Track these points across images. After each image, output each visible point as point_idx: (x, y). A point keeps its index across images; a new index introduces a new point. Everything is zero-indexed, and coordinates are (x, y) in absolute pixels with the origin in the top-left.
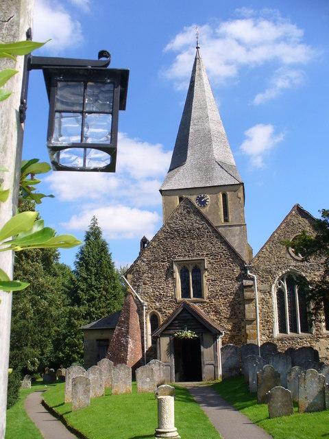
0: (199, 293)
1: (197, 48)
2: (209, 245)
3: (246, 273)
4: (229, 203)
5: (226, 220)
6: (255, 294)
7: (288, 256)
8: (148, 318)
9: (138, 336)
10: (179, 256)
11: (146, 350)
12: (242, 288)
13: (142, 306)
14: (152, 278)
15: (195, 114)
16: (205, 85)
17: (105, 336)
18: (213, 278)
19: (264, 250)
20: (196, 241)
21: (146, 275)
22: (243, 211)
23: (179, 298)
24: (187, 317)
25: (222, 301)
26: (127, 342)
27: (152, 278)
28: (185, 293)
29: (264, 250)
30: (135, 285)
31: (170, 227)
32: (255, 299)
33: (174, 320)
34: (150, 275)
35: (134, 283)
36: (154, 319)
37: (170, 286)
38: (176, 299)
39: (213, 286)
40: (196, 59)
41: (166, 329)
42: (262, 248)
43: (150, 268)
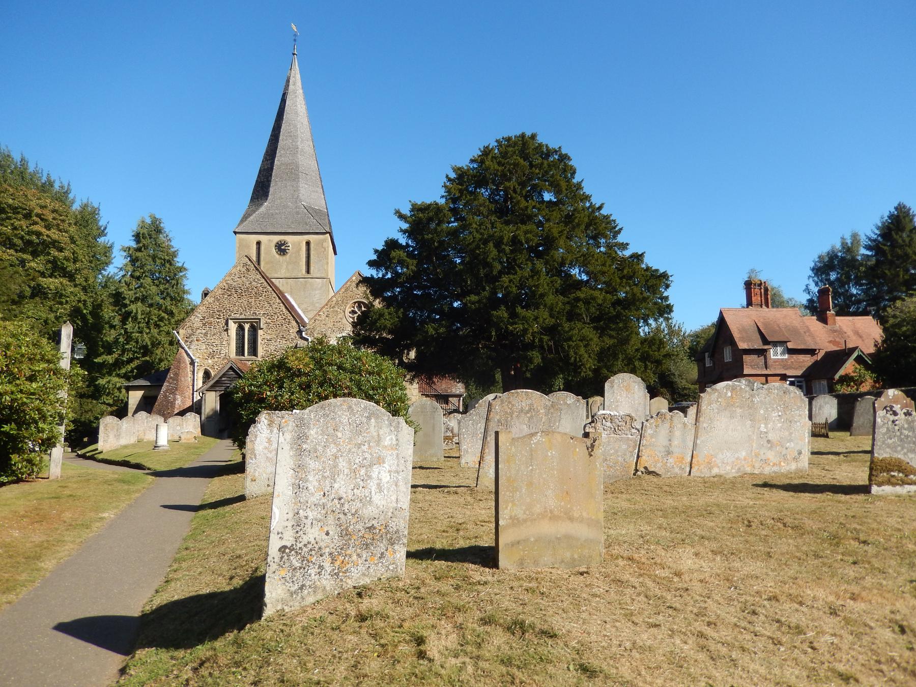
0: (254, 351)
5: (308, 272)
7: (344, 321)
14: (206, 334)
17: (152, 393)
21: (199, 331)
22: (328, 263)
26: (175, 400)
27: (206, 334)
28: (240, 351)
33: (221, 378)
36: (207, 375)
43: (204, 324)
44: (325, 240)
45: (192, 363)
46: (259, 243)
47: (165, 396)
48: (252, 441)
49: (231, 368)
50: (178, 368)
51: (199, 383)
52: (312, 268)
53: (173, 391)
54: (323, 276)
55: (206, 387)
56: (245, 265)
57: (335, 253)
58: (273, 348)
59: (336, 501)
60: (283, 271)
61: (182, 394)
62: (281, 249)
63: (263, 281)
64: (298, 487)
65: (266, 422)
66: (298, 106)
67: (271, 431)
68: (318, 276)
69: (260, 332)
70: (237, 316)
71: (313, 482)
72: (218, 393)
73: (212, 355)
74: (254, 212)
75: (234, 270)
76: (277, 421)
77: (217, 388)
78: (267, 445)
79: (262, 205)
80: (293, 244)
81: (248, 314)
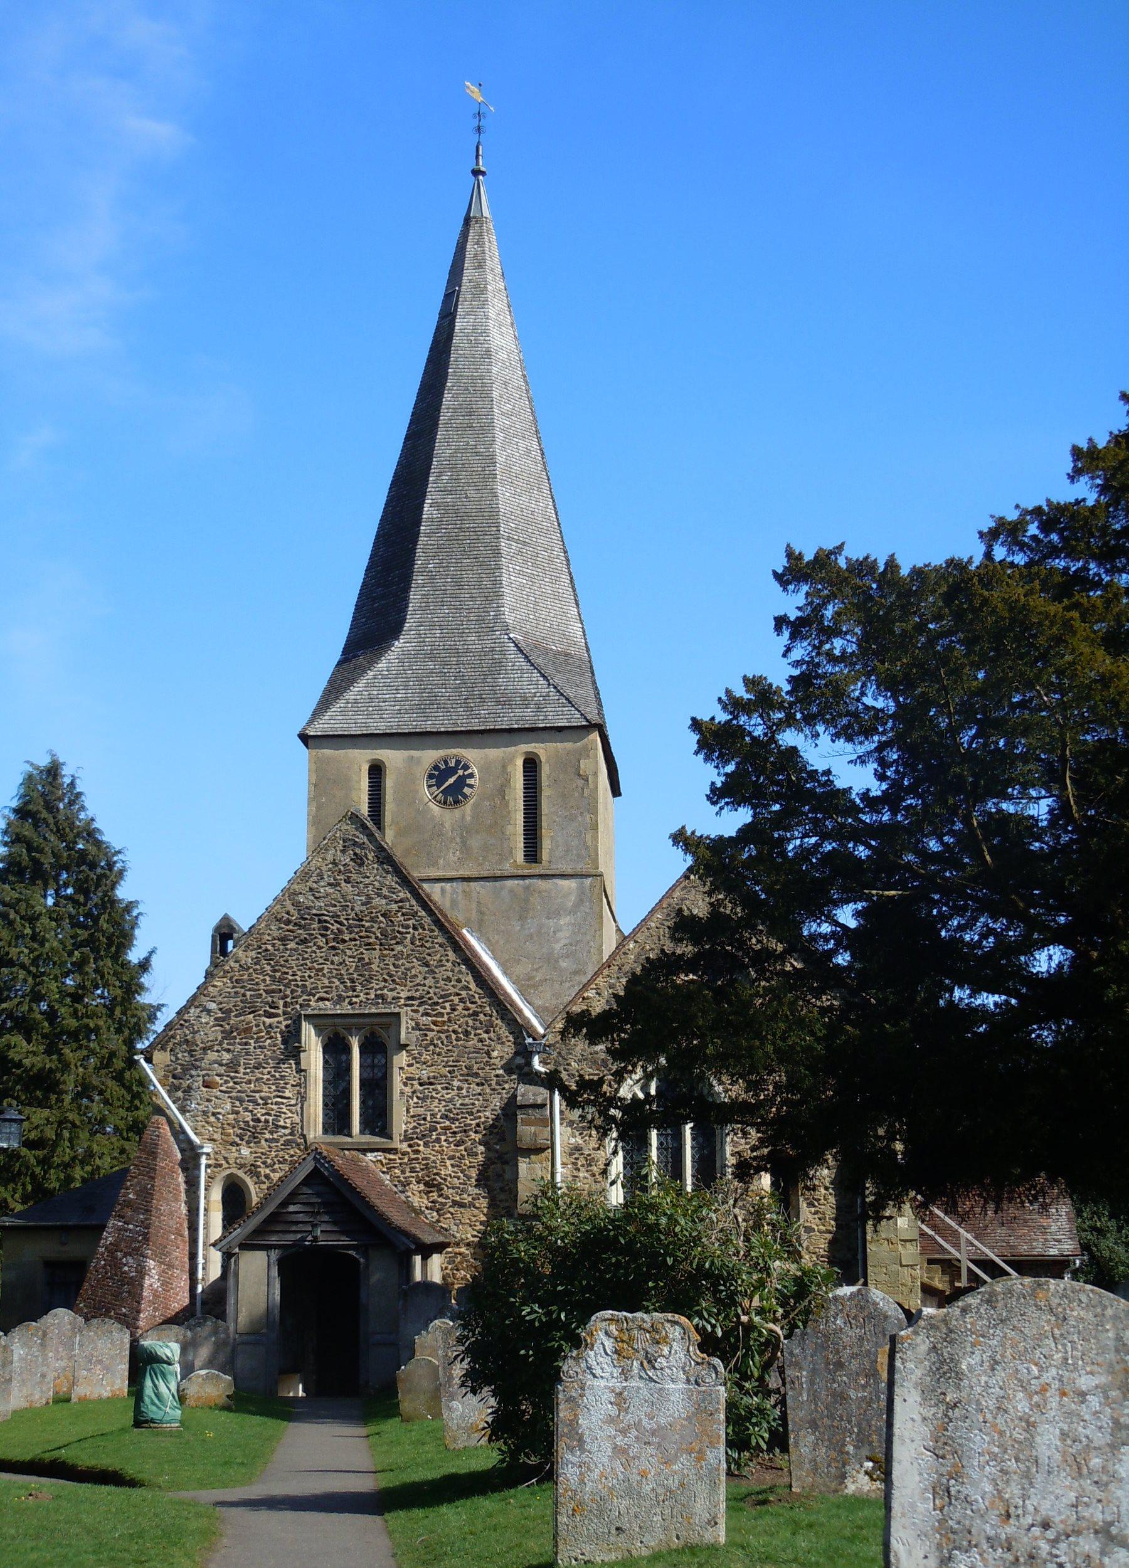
0: (378, 1119)
1: (476, 173)
2: (418, 969)
3: (529, 1063)
4: (547, 793)
6: (552, 1132)
8: (217, 1195)
9: (180, 1254)
10: (322, 999)
11: (200, 1289)
12: (511, 1109)
13: (198, 1156)
14: (233, 1066)
15: (444, 447)
16: (494, 332)
17: (73, 1250)
18: (425, 1074)
19: (590, 994)
20: (376, 954)
21: (212, 1056)
22: (595, 827)
23: (315, 1131)
24: (328, 1189)
26: (142, 1272)
27: (233, 1066)
28: (337, 1119)
29: (590, 994)
30: (177, 1089)
31: (296, 904)
32: (552, 1147)
33: (284, 1204)
34: (226, 1056)
35: (176, 1080)
37: (287, 1094)
38: (304, 1136)
39: (423, 1099)
40: (467, 221)
41: (259, 1232)
42: (585, 987)
43: (227, 1035)
44: (586, 752)
45: (190, 1157)
46: (377, 771)
47: (116, 1264)
48: (570, 1399)
50: (151, 1172)
51: (213, 1222)
52: (546, 845)
53: (138, 1244)
54: (580, 868)
55: (239, 1232)
56: (349, 843)
57: (616, 791)
58: (438, 1108)
59: (1036, 1531)
60: (453, 856)
61: (162, 1256)
62: (450, 784)
63: (404, 894)
64: (944, 1492)
65: (609, 1344)
66: (496, 328)
67: (625, 1374)
68: (567, 868)
69: (401, 1059)
70: (328, 1007)
71: (980, 1485)
72: (275, 1255)
73: (251, 1133)
74: (364, 671)
75: (317, 862)
76: (642, 1341)
77: (274, 1239)
78: (613, 1411)
79: (388, 648)
80: (485, 769)
81: (361, 1002)
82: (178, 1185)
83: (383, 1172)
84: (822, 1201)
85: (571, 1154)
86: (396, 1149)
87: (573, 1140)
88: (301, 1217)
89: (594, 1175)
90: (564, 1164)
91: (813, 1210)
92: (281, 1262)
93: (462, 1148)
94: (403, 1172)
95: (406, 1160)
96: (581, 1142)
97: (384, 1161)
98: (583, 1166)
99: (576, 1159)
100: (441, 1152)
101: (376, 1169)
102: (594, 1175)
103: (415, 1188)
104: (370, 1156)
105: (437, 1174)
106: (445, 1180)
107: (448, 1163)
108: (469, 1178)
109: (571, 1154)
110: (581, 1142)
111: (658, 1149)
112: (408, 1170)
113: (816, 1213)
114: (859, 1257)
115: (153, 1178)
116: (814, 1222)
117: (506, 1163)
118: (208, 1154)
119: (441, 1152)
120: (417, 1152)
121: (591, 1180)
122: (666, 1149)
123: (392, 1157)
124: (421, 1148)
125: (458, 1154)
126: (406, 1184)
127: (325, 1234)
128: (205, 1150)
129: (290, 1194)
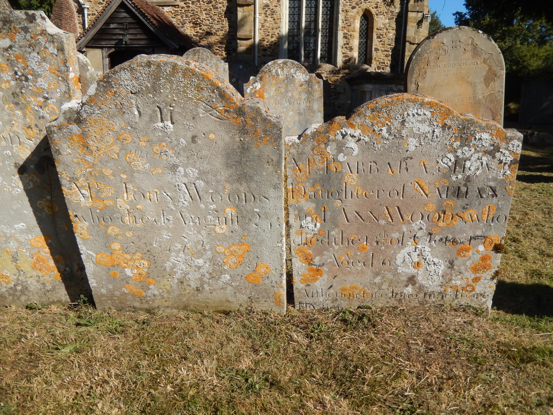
25: (204, 6)
32: (254, 4)
33: (107, 23)
45: (81, 10)
49: (122, 5)
82: (75, 24)
83: (173, 17)
84: (384, 36)
85: (264, 9)
86: (178, 5)
87: (265, 2)
88: (117, 31)
89: (274, 20)
90: (260, 14)
91: (379, 40)
92: (110, 56)
93: (210, 5)
94: (182, 17)
95: (183, 11)
96: (268, 2)
97: (173, 12)
98: (269, 15)
99: (266, 11)
100: (200, 7)
101: (170, 17)
102: (274, 20)
103: (188, 25)
104: (166, 9)
105: (199, 18)
106: (202, 21)
107: (204, 12)
108: (214, 20)
109: (264, 9)
110: (268, 2)
111: (306, 7)
112: (184, 16)
113: (381, 41)
114: (400, 63)
115: (61, 20)
116: (380, 47)
117: (232, 13)
118: (88, 9)
119: (200, 7)
120: (188, 7)
121: (273, 22)
122: (311, 7)
123: (176, 9)
124: (191, 5)
125: (208, 8)
126: (183, 24)
127: (131, 41)
128: (86, 6)
129: (109, 17)
